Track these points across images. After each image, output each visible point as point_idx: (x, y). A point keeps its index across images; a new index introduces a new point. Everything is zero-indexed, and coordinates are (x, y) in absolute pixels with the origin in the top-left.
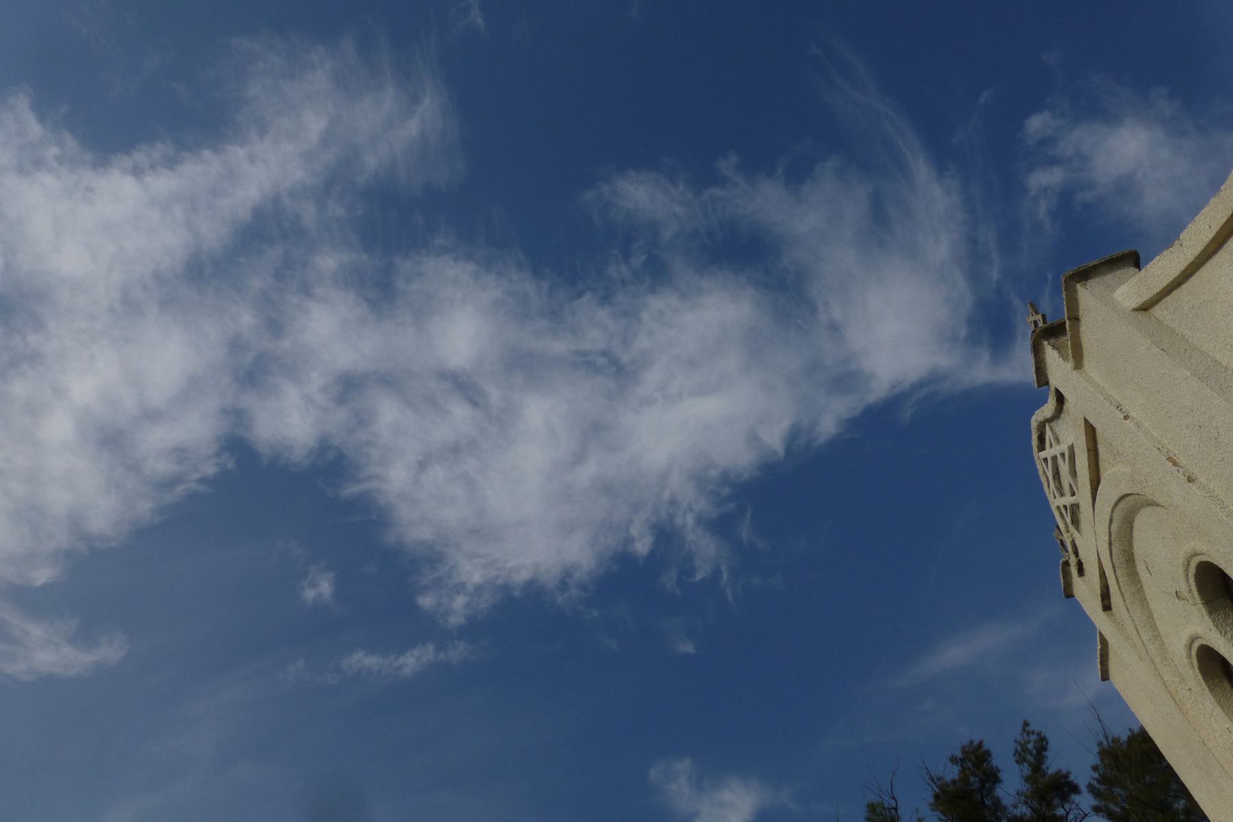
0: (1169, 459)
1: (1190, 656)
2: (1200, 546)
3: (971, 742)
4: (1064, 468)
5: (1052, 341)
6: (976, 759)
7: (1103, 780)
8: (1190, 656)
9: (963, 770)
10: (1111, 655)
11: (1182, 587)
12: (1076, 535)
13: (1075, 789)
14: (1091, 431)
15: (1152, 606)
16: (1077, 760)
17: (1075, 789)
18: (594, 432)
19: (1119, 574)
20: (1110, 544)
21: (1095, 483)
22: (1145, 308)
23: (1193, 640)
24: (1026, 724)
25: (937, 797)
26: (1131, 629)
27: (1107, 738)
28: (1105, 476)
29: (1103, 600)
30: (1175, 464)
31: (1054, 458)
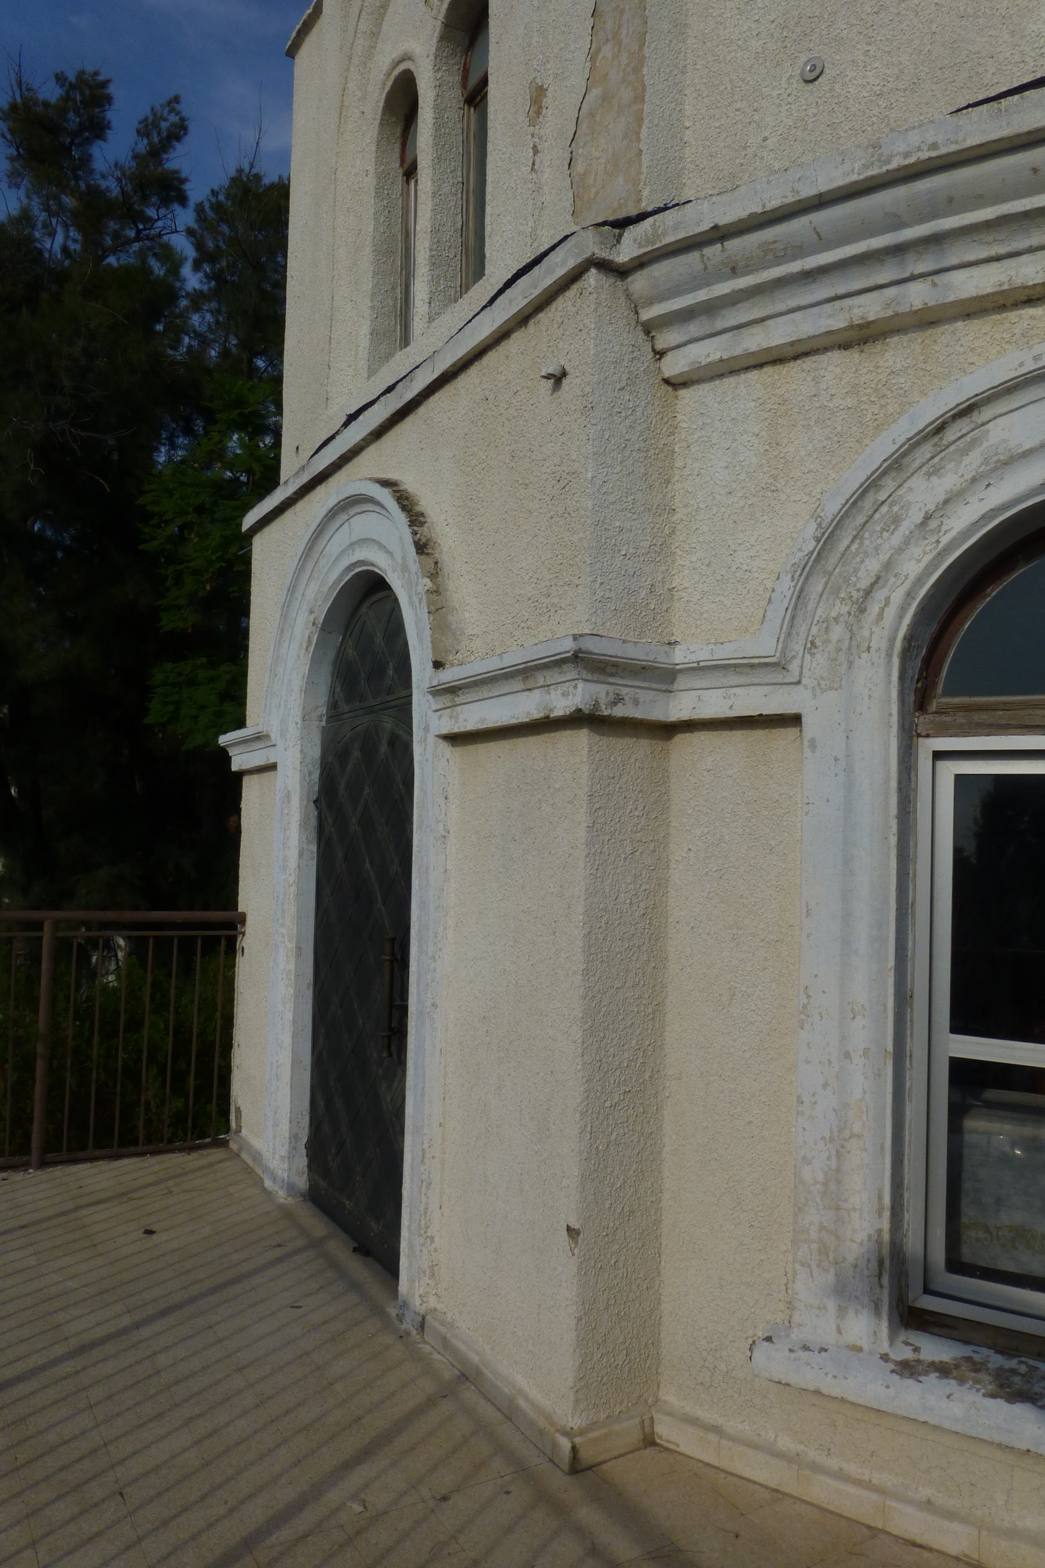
1: (389, 74)
3: (96, 74)
6: (90, 98)
7: (217, 207)
9: (66, 98)
10: (315, 31)
23: (406, 57)
25: (14, 107)
27: (252, 166)
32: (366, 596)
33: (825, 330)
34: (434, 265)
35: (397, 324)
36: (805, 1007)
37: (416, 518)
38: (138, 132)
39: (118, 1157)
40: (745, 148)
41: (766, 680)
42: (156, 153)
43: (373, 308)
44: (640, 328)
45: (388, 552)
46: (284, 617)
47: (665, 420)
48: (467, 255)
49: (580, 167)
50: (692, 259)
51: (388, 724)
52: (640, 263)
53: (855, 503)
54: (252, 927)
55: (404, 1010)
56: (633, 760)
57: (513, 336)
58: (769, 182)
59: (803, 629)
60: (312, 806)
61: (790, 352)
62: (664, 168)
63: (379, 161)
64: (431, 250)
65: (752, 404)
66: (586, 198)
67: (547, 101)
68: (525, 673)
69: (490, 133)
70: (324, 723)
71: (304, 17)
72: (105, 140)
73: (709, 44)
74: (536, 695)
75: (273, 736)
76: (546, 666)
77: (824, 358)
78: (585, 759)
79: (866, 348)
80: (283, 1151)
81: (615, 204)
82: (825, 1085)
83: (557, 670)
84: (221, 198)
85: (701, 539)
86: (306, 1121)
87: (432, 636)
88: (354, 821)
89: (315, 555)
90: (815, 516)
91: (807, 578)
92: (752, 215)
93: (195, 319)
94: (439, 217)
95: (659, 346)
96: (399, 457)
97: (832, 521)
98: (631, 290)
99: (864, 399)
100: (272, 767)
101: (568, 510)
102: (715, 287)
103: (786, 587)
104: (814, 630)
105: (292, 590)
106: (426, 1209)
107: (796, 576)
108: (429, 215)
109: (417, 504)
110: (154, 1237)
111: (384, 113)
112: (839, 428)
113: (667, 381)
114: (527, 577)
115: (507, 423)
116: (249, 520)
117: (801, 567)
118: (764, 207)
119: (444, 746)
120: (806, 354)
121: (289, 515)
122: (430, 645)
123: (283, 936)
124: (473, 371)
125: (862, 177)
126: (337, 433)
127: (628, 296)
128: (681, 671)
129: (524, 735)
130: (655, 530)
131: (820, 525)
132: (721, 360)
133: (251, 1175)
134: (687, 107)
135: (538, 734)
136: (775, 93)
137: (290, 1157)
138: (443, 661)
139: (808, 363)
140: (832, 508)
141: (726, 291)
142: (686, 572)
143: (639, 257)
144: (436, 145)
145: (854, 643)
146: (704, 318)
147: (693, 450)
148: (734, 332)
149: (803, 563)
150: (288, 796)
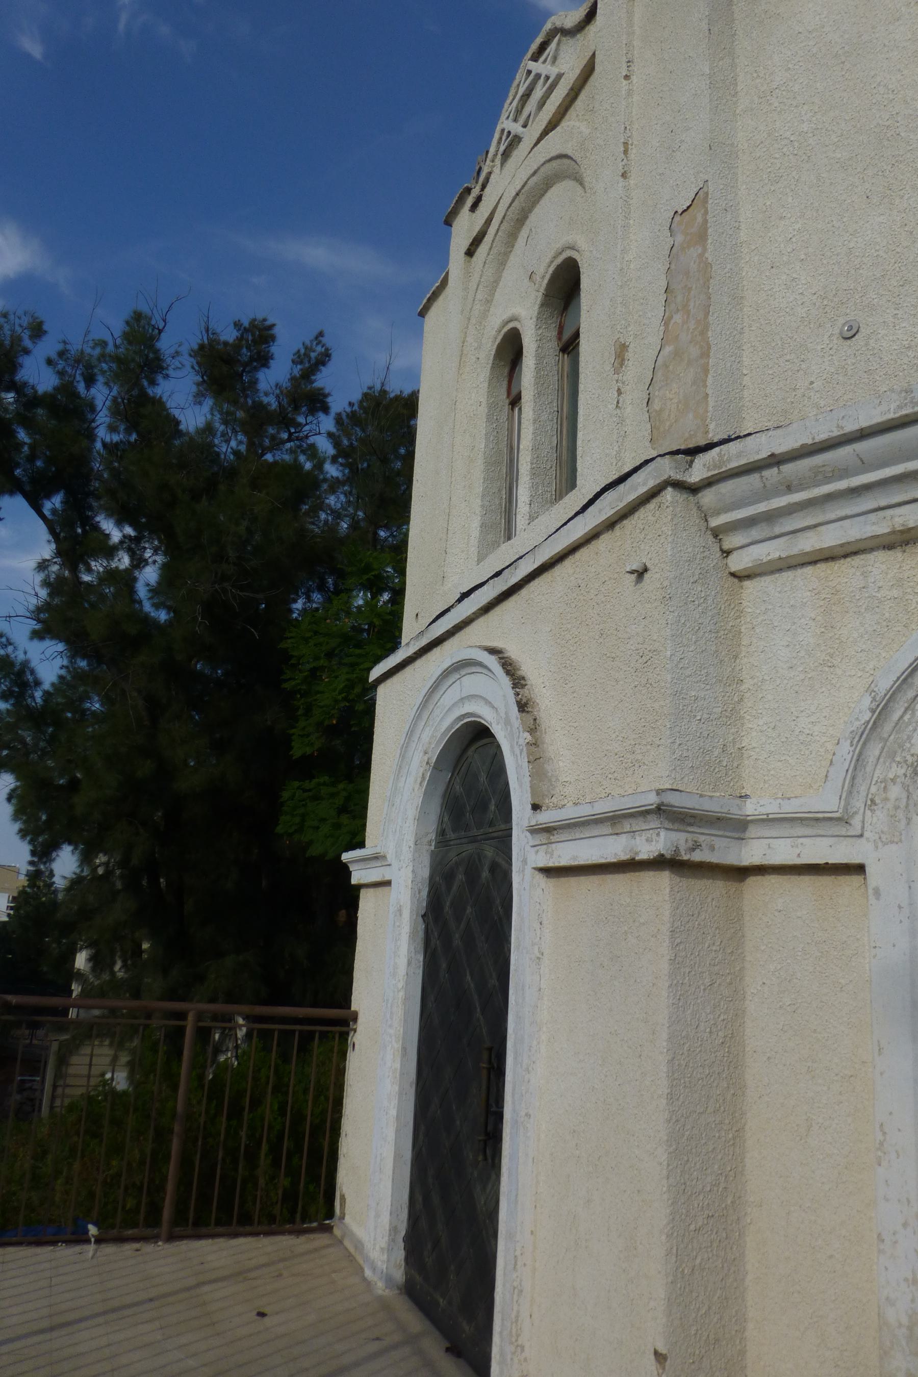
0: (625, 144)
2: (582, 242)
3: (265, 320)
4: (538, 93)
7: (352, 416)
8: (500, 331)
10: (441, 298)
11: (542, 270)
12: (497, 170)
13: (326, 409)
15: (505, 274)
16: (343, 388)
17: (326, 409)
19: (502, 228)
20: (517, 194)
21: (552, 126)
23: (513, 319)
25: (202, 347)
26: (473, 285)
27: (383, 385)
28: (564, 124)
29: (472, 244)
30: (626, 152)
31: (538, 76)
32: (473, 743)
33: (870, 535)
34: (534, 474)
35: (503, 522)
36: (881, 1144)
37: (518, 682)
38: (293, 361)
39: (236, 1235)
40: (794, 390)
41: (830, 833)
43: (483, 506)
44: (709, 532)
45: (493, 707)
46: (403, 756)
47: (732, 606)
48: (560, 466)
49: (656, 405)
50: (753, 480)
51: (489, 852)
52: (709, 483)
53: (905, 679)
54: (362, 1024)
55: (500, 1116)
56: (709, 900)
57: (602, 537)
58: (817, 420)
59: (863, 789)
60: (420, 919)
61: (841, 552)
62: (727, 406)
63: (490, 394)
64: (532, 464)
65: (809, 594)
66: (662, 429)
67: (629, 355)
68: (614, 820)
69: (582, 377)
70: (433, 848)
71: (434, 288)
72: (268, 368)
73: (762, 311)
74: (623, 839)
75: (389, 857)
76: (632, 816)
77: (871, 557)
78: (667, 898)
79: (908, 549)
80: (383, 1242)
81: (687, 435)
82: (905, 1225)
83: (641, 819)
84: (356, 407)
85: (767, 706)
86: (404, 1215)
87: (531, 782)
88: (457, 936)
89: (431, 707)
90: (870, 690)
91: (865, 744)
92: (803, 446)
93: (332, 500)
94: (538, 438)
95: (726, 546)
96: (504, 629)
97: (885, 695)
98: (701, 504)
99: (909, 590)
100: (388, 883)
101: (650, 681)
102: (773, 501)
103: (845, 751)
104: (873, 789)
105: (410, 733)
106: (517, 1317)
107: (855, 743)
108: (530, 437)
109: (519, 670)
110: (266, 1319)
112: (887, 615)
113: (733, 575)
114: (614, 736)
115: (596, 606)
116: (375, 673)
117: (859, 734)
118: (813, 439)
119: (540, 877)
120: (855, 553)
121: (408, 670)
122: (529, 789)
123: (391, 1037)
124: (568, 563)
125: (897, 415)
126: (452, 607)
127: (699, 508)
128: (752, 821)
129: (611, 873)
130: (726, 698)
131: (874, 699)
132: (780, 558)
133: (352, 1262)
134: (745, 359)
135: (624, 872)
136: (819, 348)
137: (390, 1250)
138: (540, 803)
139: (857, 560)
140: (885, 684)
141: (782, 504)
142: (754, 734)
143: (708, 478)
144: (536, 384)
145: (911, 802)
146: (763, 524)
147: (758, 631)
148: (791, 536)
149: (861, 730)
150: (400, 911)
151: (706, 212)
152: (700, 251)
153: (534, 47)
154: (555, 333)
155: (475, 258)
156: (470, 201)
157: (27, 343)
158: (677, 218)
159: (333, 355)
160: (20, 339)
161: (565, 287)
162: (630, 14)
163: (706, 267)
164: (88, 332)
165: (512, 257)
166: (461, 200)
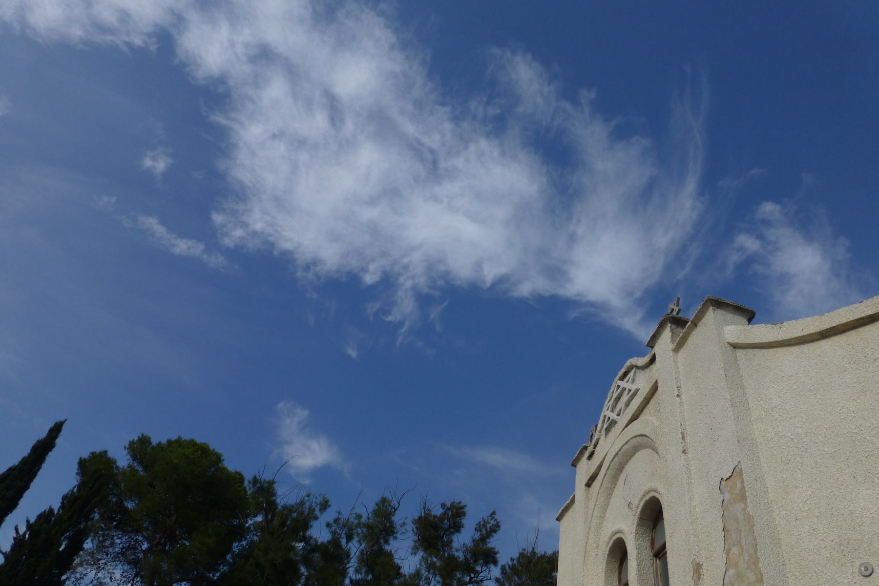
0: (682, 433)
2: (661, 489)
4: (625, 398)
5: (673, 327)
7: (513, 568)
9: (444, 514)
10: (571, 510)
11: (636, 502)
12: (603, 437)
13: (495, 562)
14: (655, 389)
16: (507, 548)
17: (495, 562)
18: (391, 193)
22: (735, 346)
24: (494, 513)
25: (420, 518)
28: (642, 417)
30: (683, 438)
31: (624, 389)
42: (484, 539)
111: (608, 557)
136: (846, 581)
144: (639, 579)
151: (743, 482)
152: (743, 506)
153: (621, 373)
154: (649, 544)
155: (591, 489)
156: (587, 454)
157: (317, 513)
158: (723, 483)
159: (502, 526)
160: (314, 510)
161: (652, 515)
162: (676, 362)
163: (749, 518)
164: (354, 508)
165: (616, 490)
166: (582, 453)
